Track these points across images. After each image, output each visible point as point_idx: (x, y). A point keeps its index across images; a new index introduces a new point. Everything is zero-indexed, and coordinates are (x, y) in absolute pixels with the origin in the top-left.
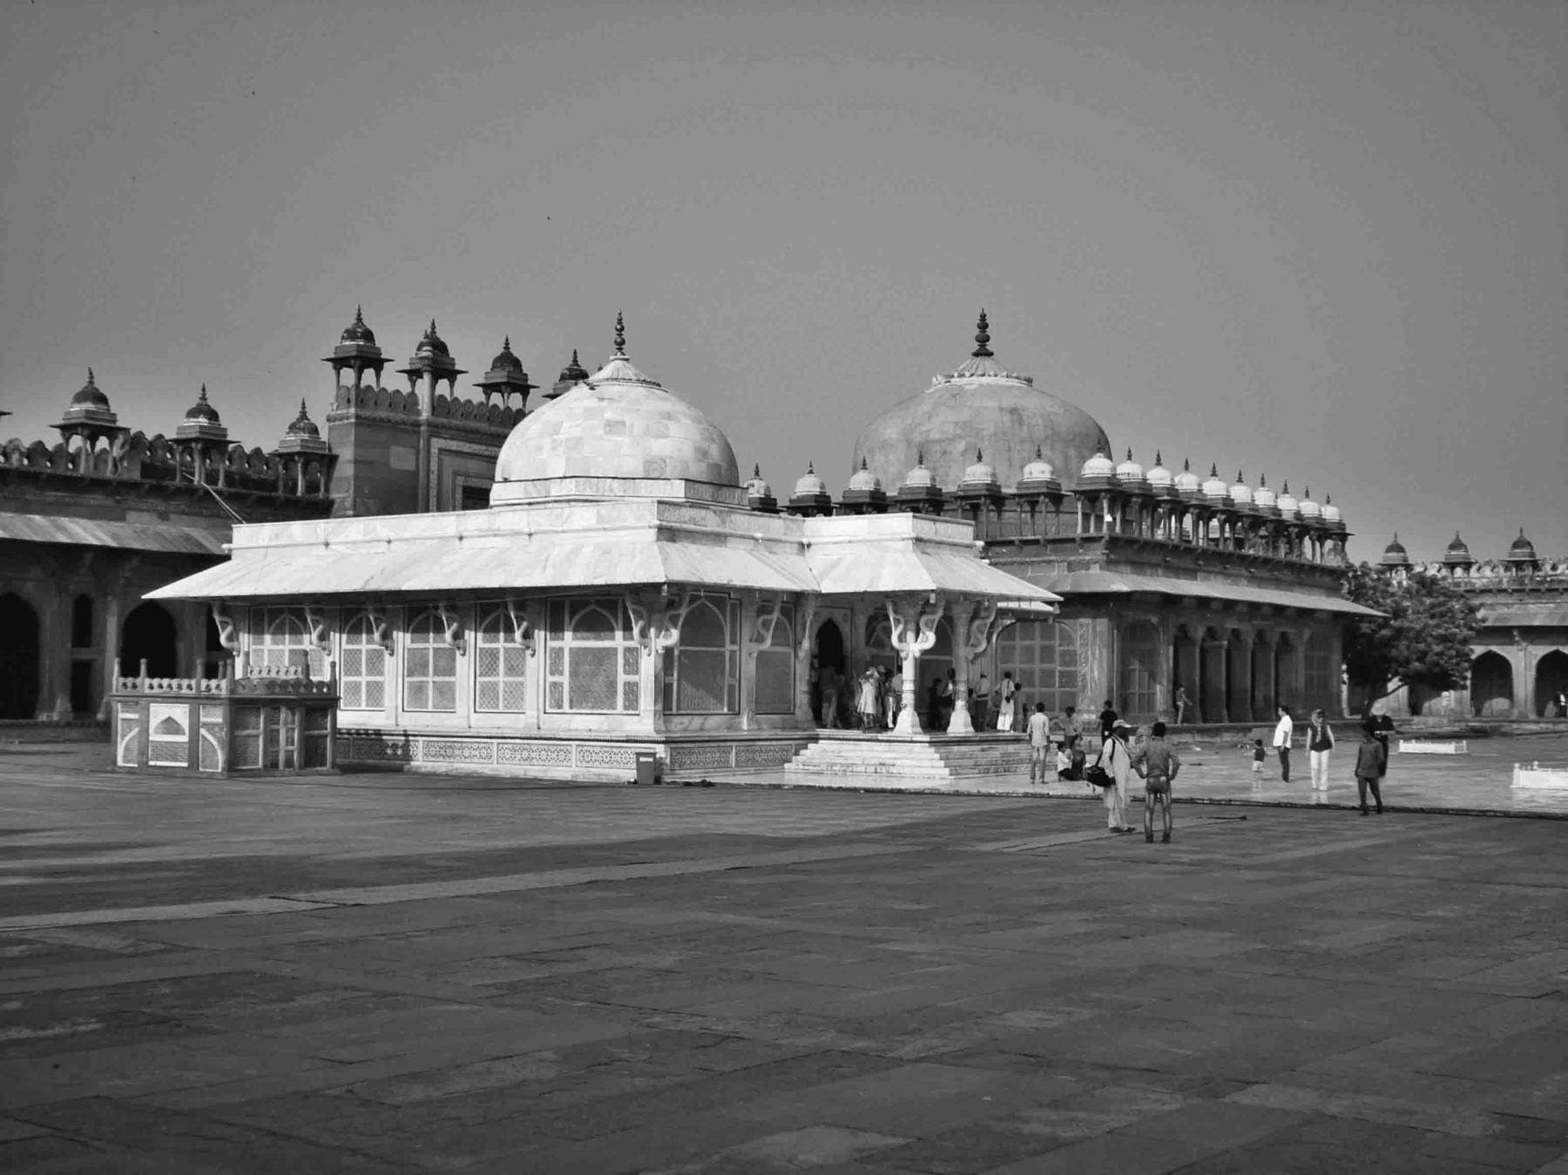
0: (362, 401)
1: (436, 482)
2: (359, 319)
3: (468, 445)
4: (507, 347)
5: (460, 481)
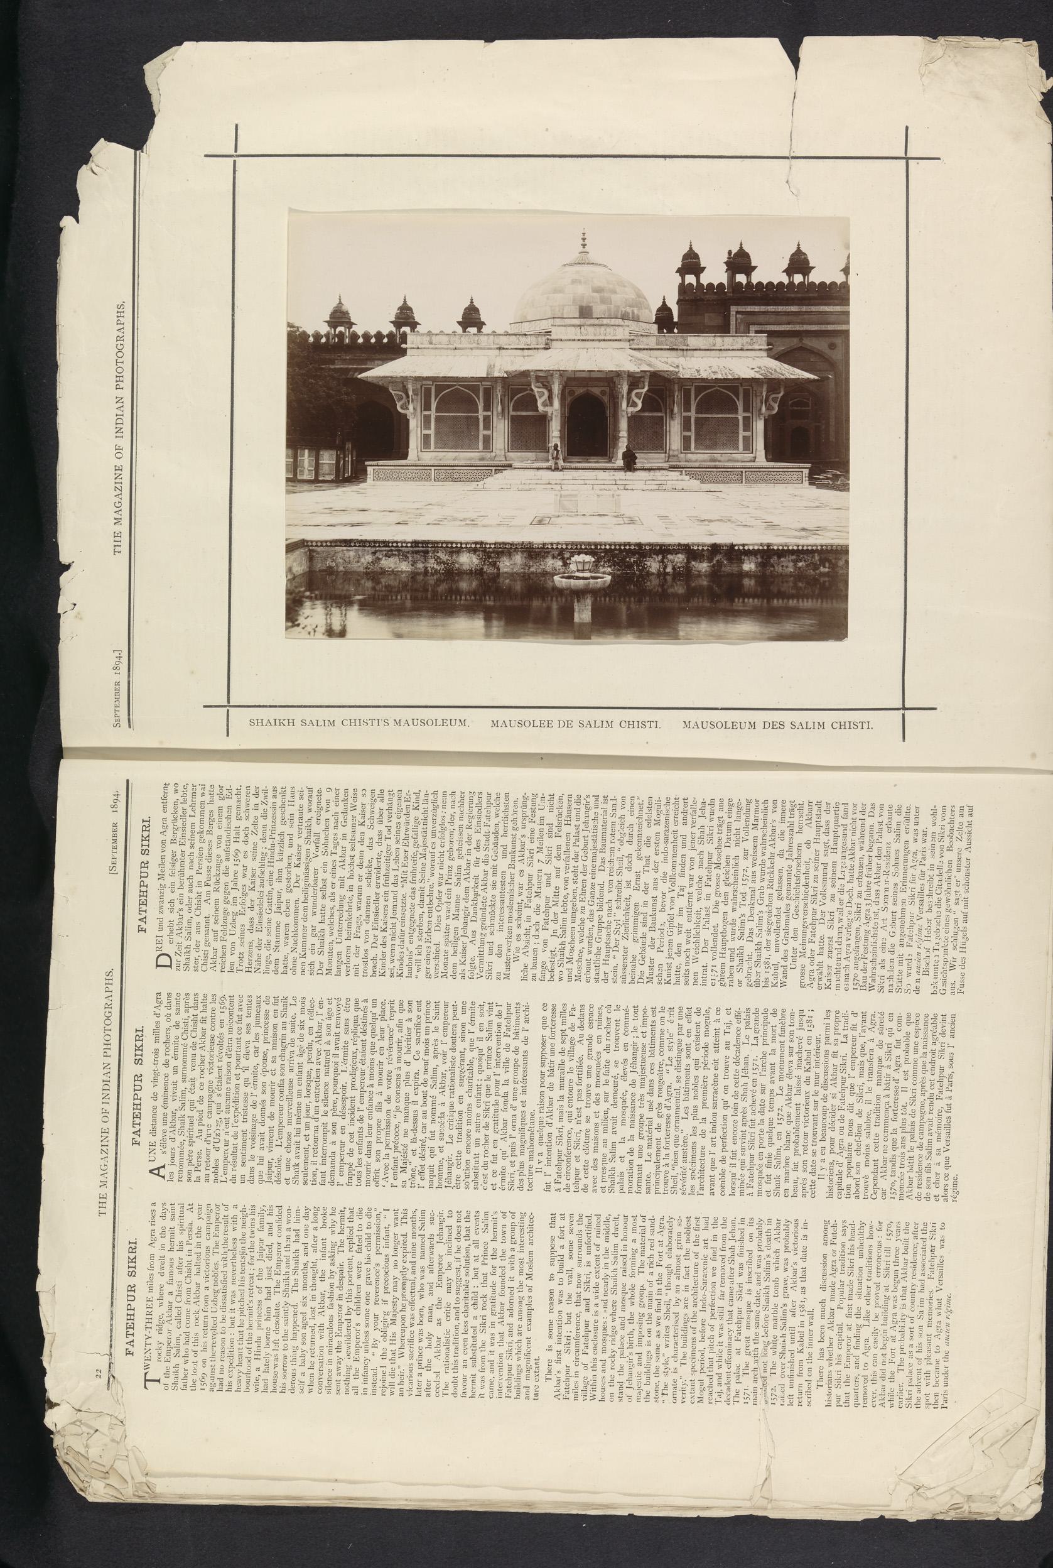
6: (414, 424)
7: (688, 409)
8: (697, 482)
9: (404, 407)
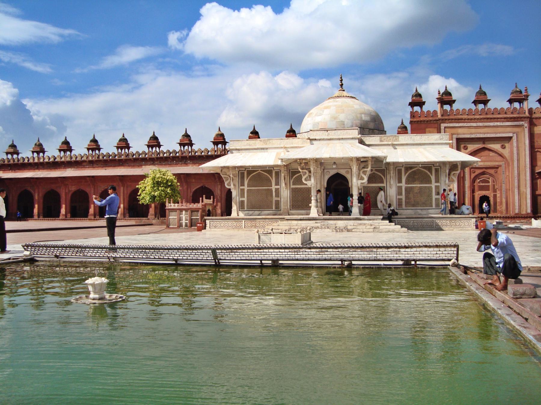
0: (414, 116)
3: (458, 124)
4: (480, 88)
5: (455, 137)
6: (234, 193)
7: (400, 181)
8: (399, 226)
9: (229, 184)
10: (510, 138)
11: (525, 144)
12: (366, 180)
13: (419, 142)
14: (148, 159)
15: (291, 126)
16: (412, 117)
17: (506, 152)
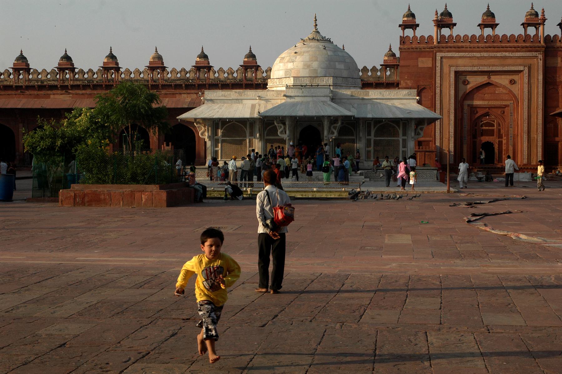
0: (404, 42)
1: (439, 70)
2: (409, 9)
4: (488, 9)
5: (453, 69)
7: (369, 134)
10: (521, 71)
11: (538, 79)
12: (336, 134)
13: (388, 97)
14: (59, 86)
15: (250, 49)
16: (402, 43)
17: (515, 89)
